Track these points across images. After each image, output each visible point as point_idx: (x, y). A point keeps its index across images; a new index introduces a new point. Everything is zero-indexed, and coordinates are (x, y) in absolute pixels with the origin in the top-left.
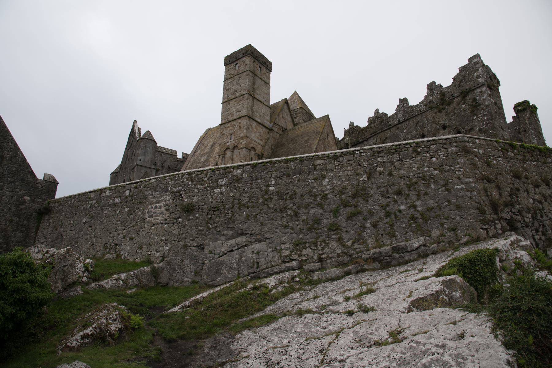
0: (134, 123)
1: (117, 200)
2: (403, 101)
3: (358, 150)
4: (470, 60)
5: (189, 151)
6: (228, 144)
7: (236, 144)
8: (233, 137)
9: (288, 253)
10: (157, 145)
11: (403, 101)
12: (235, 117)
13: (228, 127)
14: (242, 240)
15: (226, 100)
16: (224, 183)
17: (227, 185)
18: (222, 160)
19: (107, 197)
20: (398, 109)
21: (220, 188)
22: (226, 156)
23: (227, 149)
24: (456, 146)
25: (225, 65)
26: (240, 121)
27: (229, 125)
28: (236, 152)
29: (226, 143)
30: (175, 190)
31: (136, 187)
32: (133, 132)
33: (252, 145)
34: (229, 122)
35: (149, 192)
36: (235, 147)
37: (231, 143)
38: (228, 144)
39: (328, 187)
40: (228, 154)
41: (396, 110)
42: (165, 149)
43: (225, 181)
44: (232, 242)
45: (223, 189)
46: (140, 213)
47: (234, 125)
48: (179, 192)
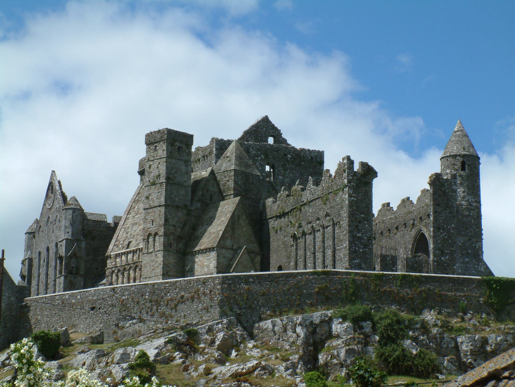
0: (52, 175)
1: (73, 301)
3: (182, 280)
5: (121, 212)
6: (150, 229)
8: (154, 224)
10: (84, 212)
14: (134, 321)
16: (127, 294)
17: (128, 295)
19: (67, 299)
22: (150, 240)
23: (150, 235)
24: (218, 280)
26: (159, 208)
27: (151, 210)
30: (104, 297)
32: (52, 186)
33: (171, 231)
35: (91, 297)
36: (156, 234)
37: (153, 230)
39: (169, 297)
40: (151, 239)
42: (94, 214)
44: (131, 322)
45: (126, 297)
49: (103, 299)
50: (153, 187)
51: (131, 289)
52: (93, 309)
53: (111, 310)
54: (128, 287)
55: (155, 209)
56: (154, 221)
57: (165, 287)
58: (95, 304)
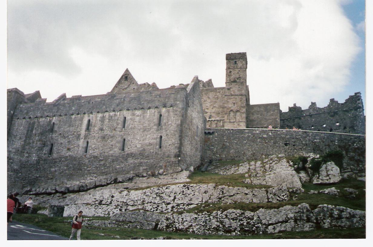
1: (265, 136)
2: (313, 104)
4: (356, 94)
7: (238, 110)
8: (236, 105)
9: (346, 166)
11: (313, 104)
12: (236, 94)
13: (232, 98)
15: (228, 81)
18: (228, 117)
20: (310, 107)
21: (317, 139)
25: (227, 59)
27: (232, 97)
28: (238, 114)
29: (231, 107)
30: (298, 137)
31: (274, 132)
32: (126, 78)
34: (232, 95)
36: (237, 111)
38: (232, 108)
40: (232, 114)
41: (309, 107)
43: (318, 137)
46: (281, 144)
47: (236, 98)
48: (299, 138)
49: (297, 138)
50: (233, 84)
51: (322, 135)
52: (286, 144)
53: (306, 148)
54: (318, 133)
55: (237, 97)
56: (235, 104)
57: (351, 139)
58: (289, 141)
